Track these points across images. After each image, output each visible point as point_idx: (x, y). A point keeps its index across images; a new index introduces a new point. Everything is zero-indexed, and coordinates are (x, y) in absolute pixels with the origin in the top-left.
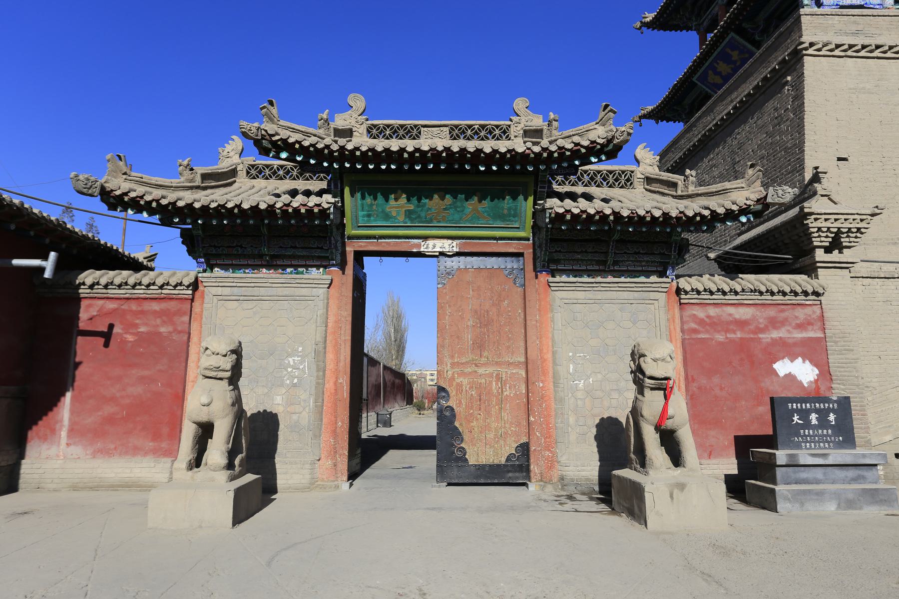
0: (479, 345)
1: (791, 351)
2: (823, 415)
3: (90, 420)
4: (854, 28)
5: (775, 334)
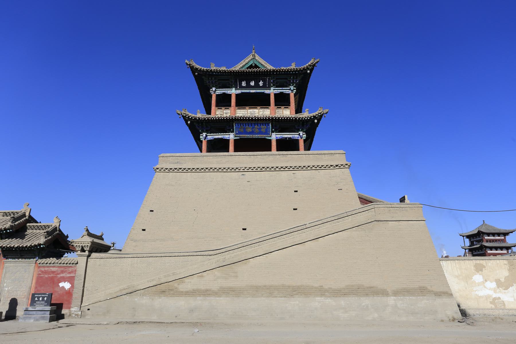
1: (64, 280)
2: (43, 298)
4: (176, 161)
5: (62, 275)
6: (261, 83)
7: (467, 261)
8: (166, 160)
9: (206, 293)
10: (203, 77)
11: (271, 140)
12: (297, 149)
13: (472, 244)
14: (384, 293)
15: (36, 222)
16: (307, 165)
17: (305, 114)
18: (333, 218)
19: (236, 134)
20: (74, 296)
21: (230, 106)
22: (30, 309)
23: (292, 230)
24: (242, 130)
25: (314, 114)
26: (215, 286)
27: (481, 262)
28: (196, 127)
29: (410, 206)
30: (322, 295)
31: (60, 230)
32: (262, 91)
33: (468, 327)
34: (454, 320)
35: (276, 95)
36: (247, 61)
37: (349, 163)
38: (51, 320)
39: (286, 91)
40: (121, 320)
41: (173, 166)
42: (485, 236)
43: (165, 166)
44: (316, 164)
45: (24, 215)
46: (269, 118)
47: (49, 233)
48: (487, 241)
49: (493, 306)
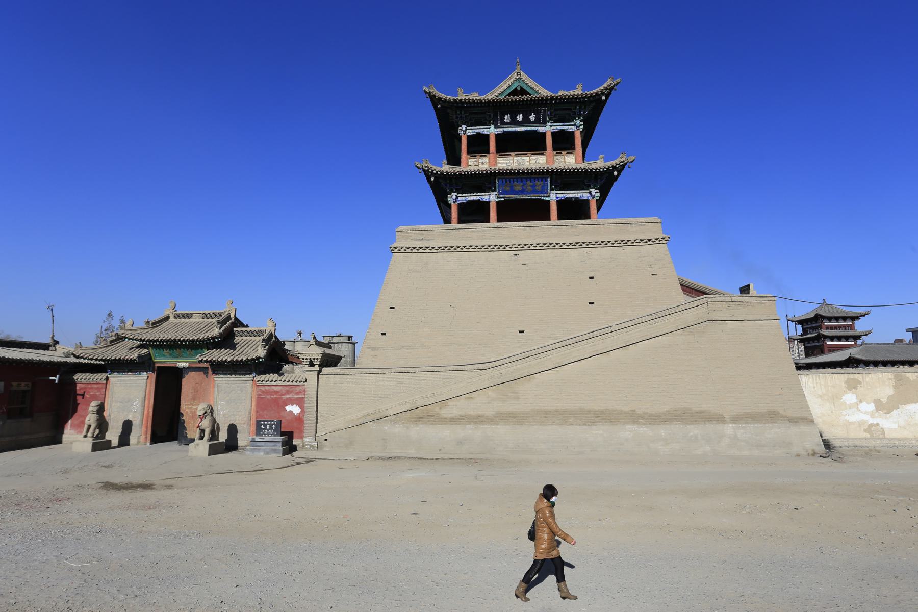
0: (194, 399)
1: (292, 402)
2: (271, 426)
3: (76, 422)
4: (421, 237)
6: (532, 117)
7: (836, 376)
9: (478, 420)
11: (548, 202)
12: (587, 216)
13: (805, 332)
14: (719, 419)
15: (244, 326)
16: (606, 240)
17: (599, 164)
19: (500, 194)
20: (306, 423)
21: (488, 151)
22: (257, 439)
24: (508, 188)
25: (613, 163)
26: (489, 411)
27: (856, 376)
28: (441, 186)
29: (758, 299)
31: (276, 337)
32: (534, 129)
33: (836, 464)
34: (814, 454)
35: (553, 133)
37: (667, 236)
38: (285, 453)
40: (373, 455)
43: (406, 244)
44: (619, 239)
45: (229, 318)
46: (548, 171)
47: (266, 341)
48: (827, 328)
49: (868, 435)
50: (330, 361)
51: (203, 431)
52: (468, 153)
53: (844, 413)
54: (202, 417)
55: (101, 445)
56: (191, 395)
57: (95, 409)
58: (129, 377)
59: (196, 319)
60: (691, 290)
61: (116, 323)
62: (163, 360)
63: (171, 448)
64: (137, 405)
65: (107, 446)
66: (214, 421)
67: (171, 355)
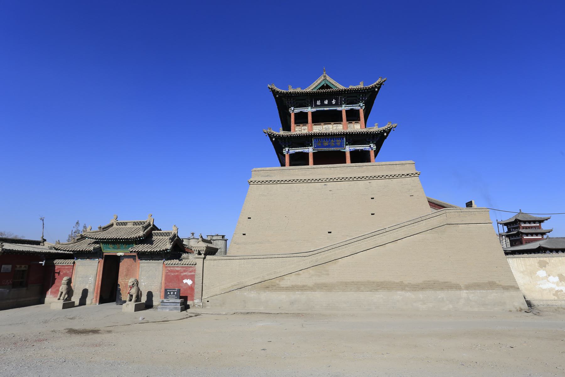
0: (127, 275)
1: (187, 277)
2: (174, 292)
3: (54, 290)
6: (334, 102)
7: (531, 259)
8: (258, 174)
9: (303, 288)
10: (283, 99)
11: (345, 152)
12: (369, 160)
13: (509, 230)
14: (457, 287)
15: (158, 230)
17: (375, 129)
18: (410, 223)
19: (315, 148)
20: (196, 290)
21: (307, 122)
22: (165, 301)
23: (373, 234)
24: (320, 144)
25: (384, 128)
27: (545, 259)
28: (279, 144)
29: (478, 210)
30: (403, 289)
31: (178, 237)
33: (536, 317)
35: (347, 111)
36: (319, 82)
37: (418, 172)
38: (182, 310)
39: (356, 107)
40: (236, 311)
41: (265, 179)
42: (521, 223)
44: (389, 174)
45: (149, 225)
46: (344, 133)
47: (172, 239)
48: (523, 228)
49: (556, 298)
50: (211, 251)
51: (132, 296)
52: (295, 123)
53: (539, 283)
54: (131, 287)
55: (68, 305)
56: (125, 273)
57: (66, 282)
58: (87, 262)
59: (130, 226)
60: (435, 205)
61: (81, 228)
62: (109, 251)
63: (112, 306)
64: (91, 279)
65: (72, 305)
66: (138, 290)
67: (113, 248)
